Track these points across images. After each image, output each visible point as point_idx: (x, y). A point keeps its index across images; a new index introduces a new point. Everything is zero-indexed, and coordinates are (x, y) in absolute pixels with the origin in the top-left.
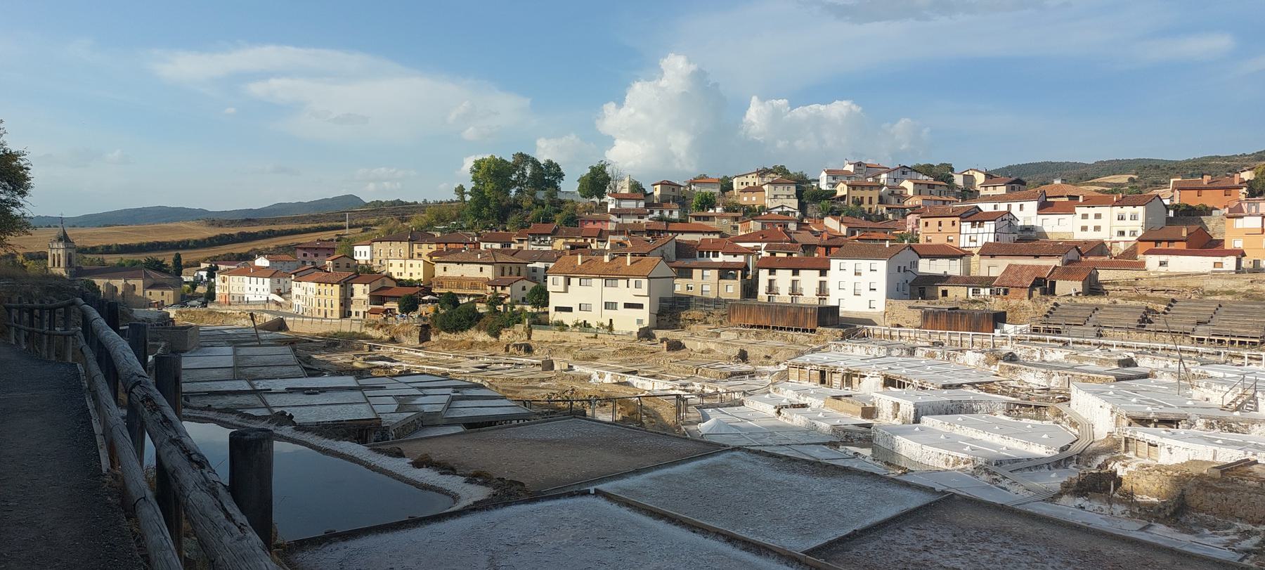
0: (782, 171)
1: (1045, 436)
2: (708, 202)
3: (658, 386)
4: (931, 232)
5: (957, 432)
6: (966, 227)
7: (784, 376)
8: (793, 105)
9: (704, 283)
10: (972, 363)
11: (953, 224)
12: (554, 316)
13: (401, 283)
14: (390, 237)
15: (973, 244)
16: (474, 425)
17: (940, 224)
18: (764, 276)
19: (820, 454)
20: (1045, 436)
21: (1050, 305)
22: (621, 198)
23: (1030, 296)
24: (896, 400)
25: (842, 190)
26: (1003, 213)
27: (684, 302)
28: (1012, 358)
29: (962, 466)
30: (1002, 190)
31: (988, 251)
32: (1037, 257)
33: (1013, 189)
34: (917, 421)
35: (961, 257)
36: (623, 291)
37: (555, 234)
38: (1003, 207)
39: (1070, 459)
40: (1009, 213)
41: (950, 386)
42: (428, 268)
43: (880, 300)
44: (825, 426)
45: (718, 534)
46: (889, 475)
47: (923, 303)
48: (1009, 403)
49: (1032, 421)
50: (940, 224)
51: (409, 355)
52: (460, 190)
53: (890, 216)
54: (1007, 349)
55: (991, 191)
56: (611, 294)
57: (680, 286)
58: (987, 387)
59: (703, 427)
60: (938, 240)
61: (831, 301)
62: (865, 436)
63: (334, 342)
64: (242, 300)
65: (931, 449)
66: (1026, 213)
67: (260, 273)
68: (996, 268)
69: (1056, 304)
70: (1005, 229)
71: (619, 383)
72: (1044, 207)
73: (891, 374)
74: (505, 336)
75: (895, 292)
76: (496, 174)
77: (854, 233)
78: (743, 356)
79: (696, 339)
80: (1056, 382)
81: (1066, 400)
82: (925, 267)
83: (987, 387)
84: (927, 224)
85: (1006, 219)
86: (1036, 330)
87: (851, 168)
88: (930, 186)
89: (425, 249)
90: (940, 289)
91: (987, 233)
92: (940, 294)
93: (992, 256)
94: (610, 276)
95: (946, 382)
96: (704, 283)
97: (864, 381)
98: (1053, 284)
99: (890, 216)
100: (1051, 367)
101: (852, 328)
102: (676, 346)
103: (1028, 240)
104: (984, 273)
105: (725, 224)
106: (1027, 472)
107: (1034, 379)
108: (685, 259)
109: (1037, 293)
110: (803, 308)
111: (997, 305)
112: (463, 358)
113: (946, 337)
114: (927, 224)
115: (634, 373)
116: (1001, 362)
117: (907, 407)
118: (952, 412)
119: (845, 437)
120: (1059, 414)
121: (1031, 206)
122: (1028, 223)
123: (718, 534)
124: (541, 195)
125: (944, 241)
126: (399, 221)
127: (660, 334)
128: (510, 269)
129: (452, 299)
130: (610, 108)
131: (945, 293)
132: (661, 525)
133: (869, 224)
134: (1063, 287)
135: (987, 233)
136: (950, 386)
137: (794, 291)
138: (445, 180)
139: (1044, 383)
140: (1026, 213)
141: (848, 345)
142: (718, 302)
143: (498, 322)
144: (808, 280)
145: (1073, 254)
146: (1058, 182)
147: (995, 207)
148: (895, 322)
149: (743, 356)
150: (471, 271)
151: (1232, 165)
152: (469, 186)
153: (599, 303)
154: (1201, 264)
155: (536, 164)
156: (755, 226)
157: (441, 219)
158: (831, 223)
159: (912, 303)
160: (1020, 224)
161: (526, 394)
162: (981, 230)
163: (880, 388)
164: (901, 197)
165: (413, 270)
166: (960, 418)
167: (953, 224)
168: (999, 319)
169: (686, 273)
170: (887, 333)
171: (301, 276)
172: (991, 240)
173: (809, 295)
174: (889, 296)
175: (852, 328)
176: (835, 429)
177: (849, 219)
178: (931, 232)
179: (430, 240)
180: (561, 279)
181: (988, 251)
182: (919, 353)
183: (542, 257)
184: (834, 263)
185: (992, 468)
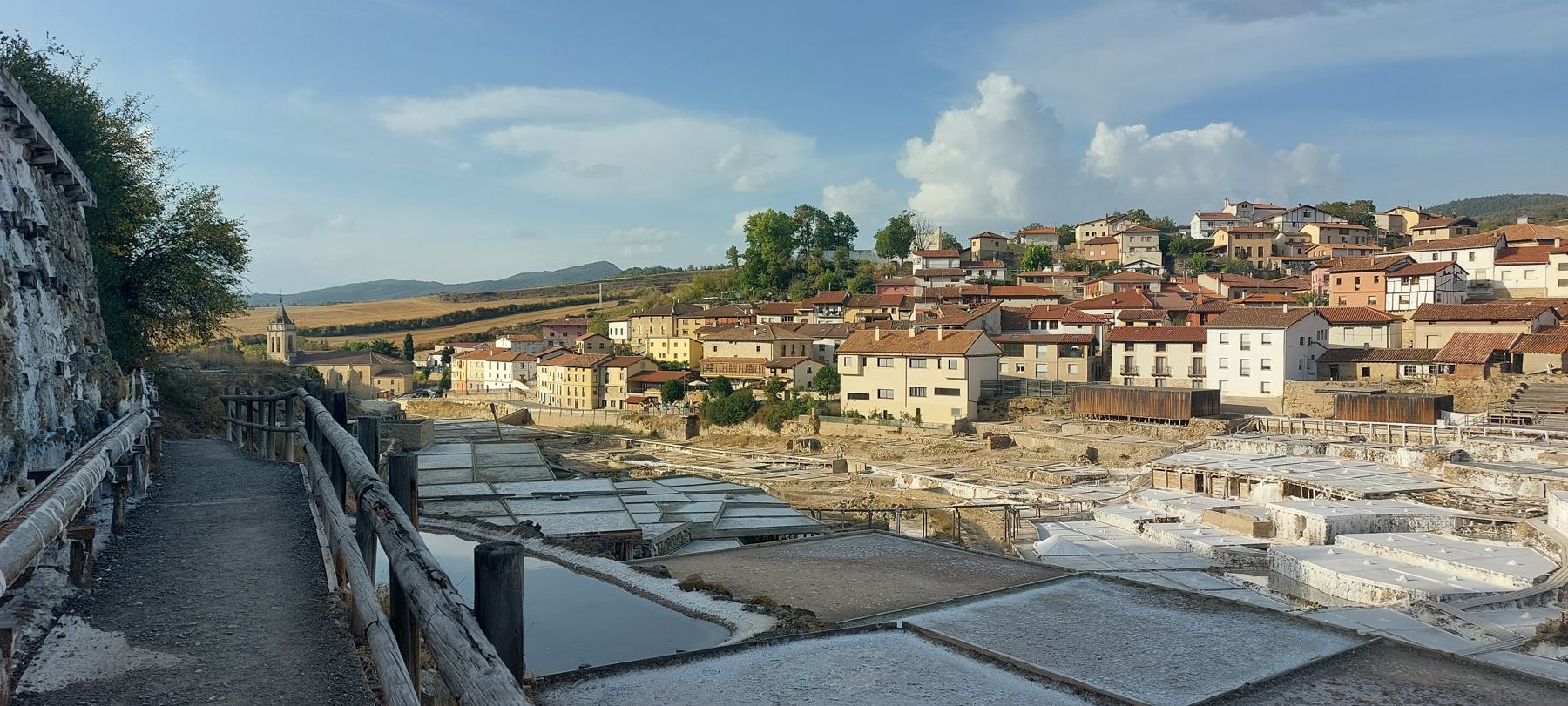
0: (1141, 216)
1: (1512, 563)
2: (1043, 258)
3: (982, 494)
4: (1345, 292)
5: (1386, 556)
6: (1395, 284)
7: (1148, 481)
8: (1153, 131)
9: (1038, 362)
10: (1405, 464)
11: (1376, 280)
12: (847, 405)
13: (663, 366)
14: (651, 311)
15: (1405, 307)
16: (751, 539)
17: (1358, 281)
18: (1118, 351)
19: (1197, 583)
20: (1512, 563)
21: (1515, 386)
22: (929, 256)
23: (1487, 375)
24: (1301, 513)
25: (1221, 239)
26: (1447, 265)
27: (1013, 387)
28: (1462, 457)
29: (1394, 601)
30: (1443, 234)
31: (1426, 316)
32: (1495, 322)
33: (1459, 232)
34: (1330, 541)
35: (1388, 323)
36: (933, 374)
37: (846, 303)
38: (1445, 257)
39: (1549, 593)
40: (1454, 264)
41: (1376, 496)
42: (696, 346)
43: (1276, 383)
44: (1203, 546)
45: (1063, 683)
46: (1294, 613)
47: (1336, 386)
48: (1460, 518)
49: (1492, 543)
50: (1358, 281)
51: (674, 453)
52: (733, 253)
53: (1289, 272)
54: (1455, 445)
55: (1427, 236)
56: (918, 377)
57: (1008, 366)
58: (1427, 496)
59: (1041, 547)
60: (1356, 301)
61: (1210, 384)
62: (1258, 561)
63: (586, 438)
64: (482, 389)
65: (1350, 578)
66: (1479, 264)
67: (501, 355)
68: (1439, 337)
69: (1524, 385)
70: (1449, 286)
71: (930, 490)
72: (1505, 255)
73: (1293, 478)
74: (788, 429)
75: (1297, 370)
76: (775, 231)
77: (1238, 295)
78: (1092, 456)
79: (1029, 434)
80: (1526, 490)
81: (1541, 514)
82: (1338, 337)
83: (1427, 496)
84: (1339, 281)
85: (1452, 272)
86: (1495, 420)
87: (1233, 211)
88: (1342, 231)
89: (692, 325)
90: (1360, 366)
91: (1423, 292)
92: (1360, 373)
93: (1432, 322)
95: (1369, 490)
96: (1038, 362)
97: (1257, 489)
98: (1519, 358)
99: (1289, 272)
100: (1520, 470)
102: (1003, 443)
103: (1483, 300)
104: (1420, 345)
105: (1065, 286)
106: (1487, 610)
107: (1494, 486)
108: (1014, 331)
109: (1496, 370)
110: (1171, 394)
111: (1439, 386)
112: (739, 456)
113: (1370, 430)
114: (1339, 281)
115: (950, 476)
116: (1447, 464)
117: (1317, 524)
118: (1379, 530)
119: (1232, 561)
120: (1531, 533)
121: (1486, 255)
122: (1481, 278)
123: (1063, 683)
124: (829, 256)
125: (1365, 304)
126: (661, 291)
127: (982, 427)
128: (793, 347)
129: (724, 385)
130: (915, 144)
131: (1366, 372)
132: (988, 670)
133: (1259, 283)
134: (1531, 361)
135: (1423, 292)
136: (1376, 496)
137: (1159, 371)
138: (717, 242)
139: (1509, 491)
140: (1479, 264)
141: (1233, 441)
142: (1058, 386)
143: (780, 412)
144: (1178, 357)
145: (1547, 318)
146: (1522, 221)
147: (1435, 257)
148: (1298, 411)
149: (1092, 456)
150: (746, 351)
152: (743, 247)
153: (905, 389)
155: (822, 217)
156: (1106, 288)
157: (710, 288)
158: (1207, 282)
159: (1321, 385)
160: (1469, 278)
161: (815, 502)
162: (1415, 288)
163: (1279, 498)
164: (1303, 245)
165: (679, 351)
166: (1390, 537)
167: (1376, 280)
168: (1443, 405)
169: (1015, 349)
170: (1287, 425)
171: (547, 359)
172: (1430, 300)
174: (1289, 376)
176: (1218, 551)
177: (1231, 277)
178: (1345, 292)
179: (698, 313)
180: (855, 359)
181: (1426, 316)
182: (1331, 450)
183: (831, 331)
184: (1213, 335)
185: (1437, 605)
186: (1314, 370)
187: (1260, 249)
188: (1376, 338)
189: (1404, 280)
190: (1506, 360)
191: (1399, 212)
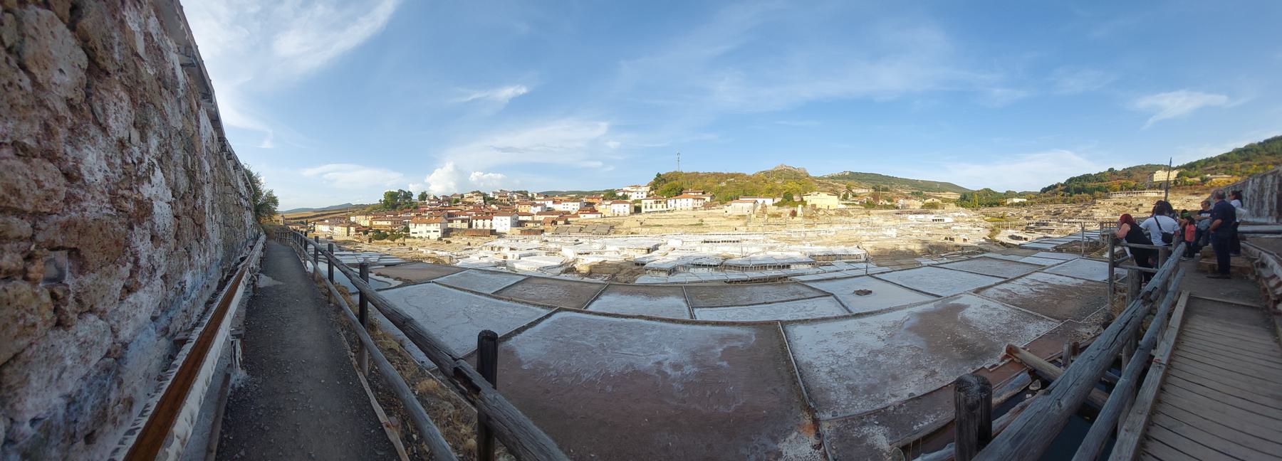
9: (457, 224)
27: (451, 230)
36: (432, 227)
57: (450, 225)
68: (542, 218)
94: (428, 223)
96: (457, 224)
101: (500, 235)
108: (451, 218)
144: (488, 222)
150: (385, 223)
151: (599, 193)
153: (425, 232)
154: (593, 216)
165: (367, 223)
168: (543, 231)
173: (488, 227)
175: (500, 235)
181: (539, 214)
188: (529, 218)
190: (554, 222)
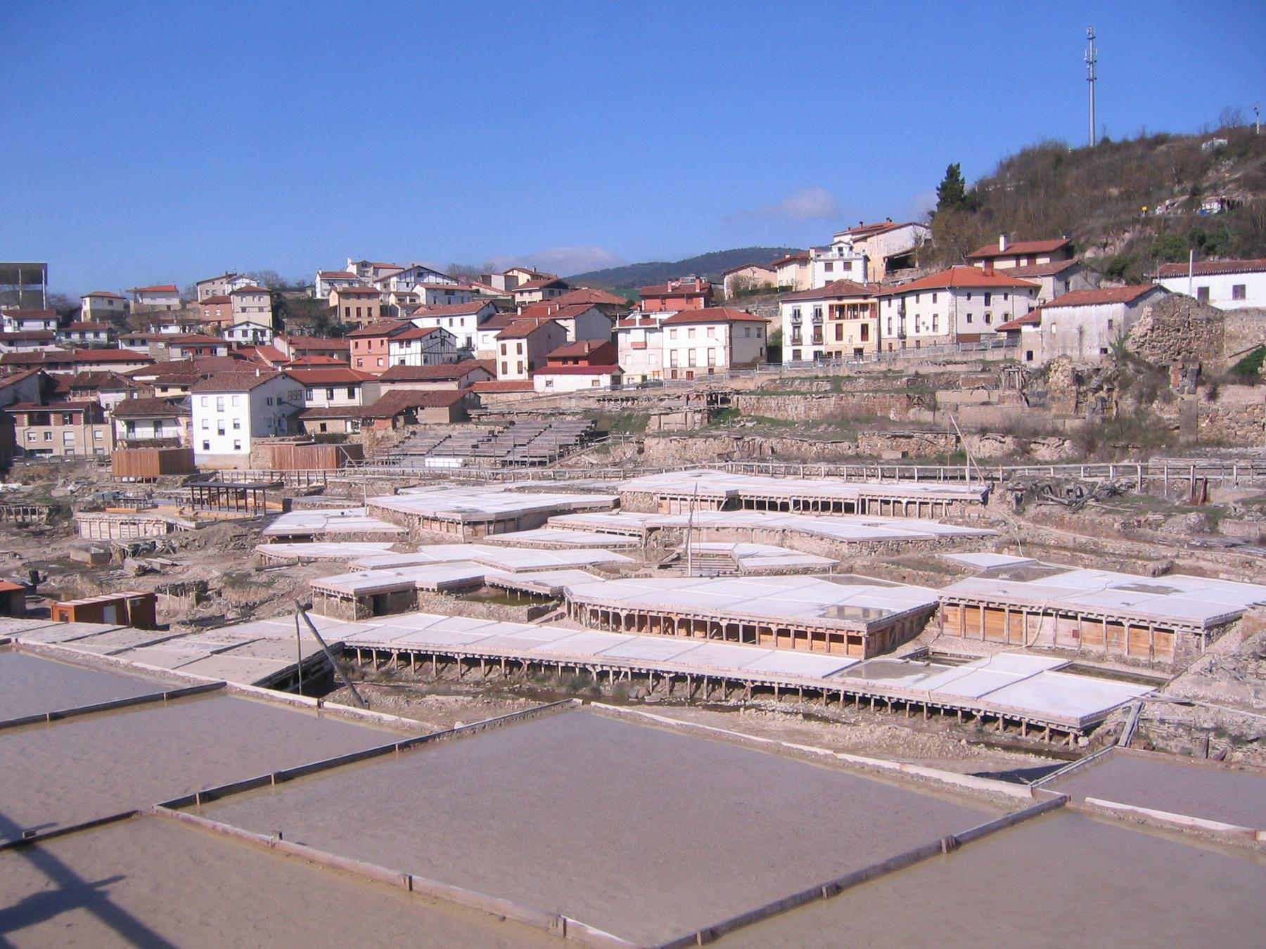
6: (395, 347)
23: (394, 427)
32: (435, 381)
33: (551, 293)
85: (440, 338)
91: (413, 355)
162: (408, 350)
174: (257, 432)
186: (285, 425)
187: (359, 309)
189: (401, 347)
191: (516, 273)
